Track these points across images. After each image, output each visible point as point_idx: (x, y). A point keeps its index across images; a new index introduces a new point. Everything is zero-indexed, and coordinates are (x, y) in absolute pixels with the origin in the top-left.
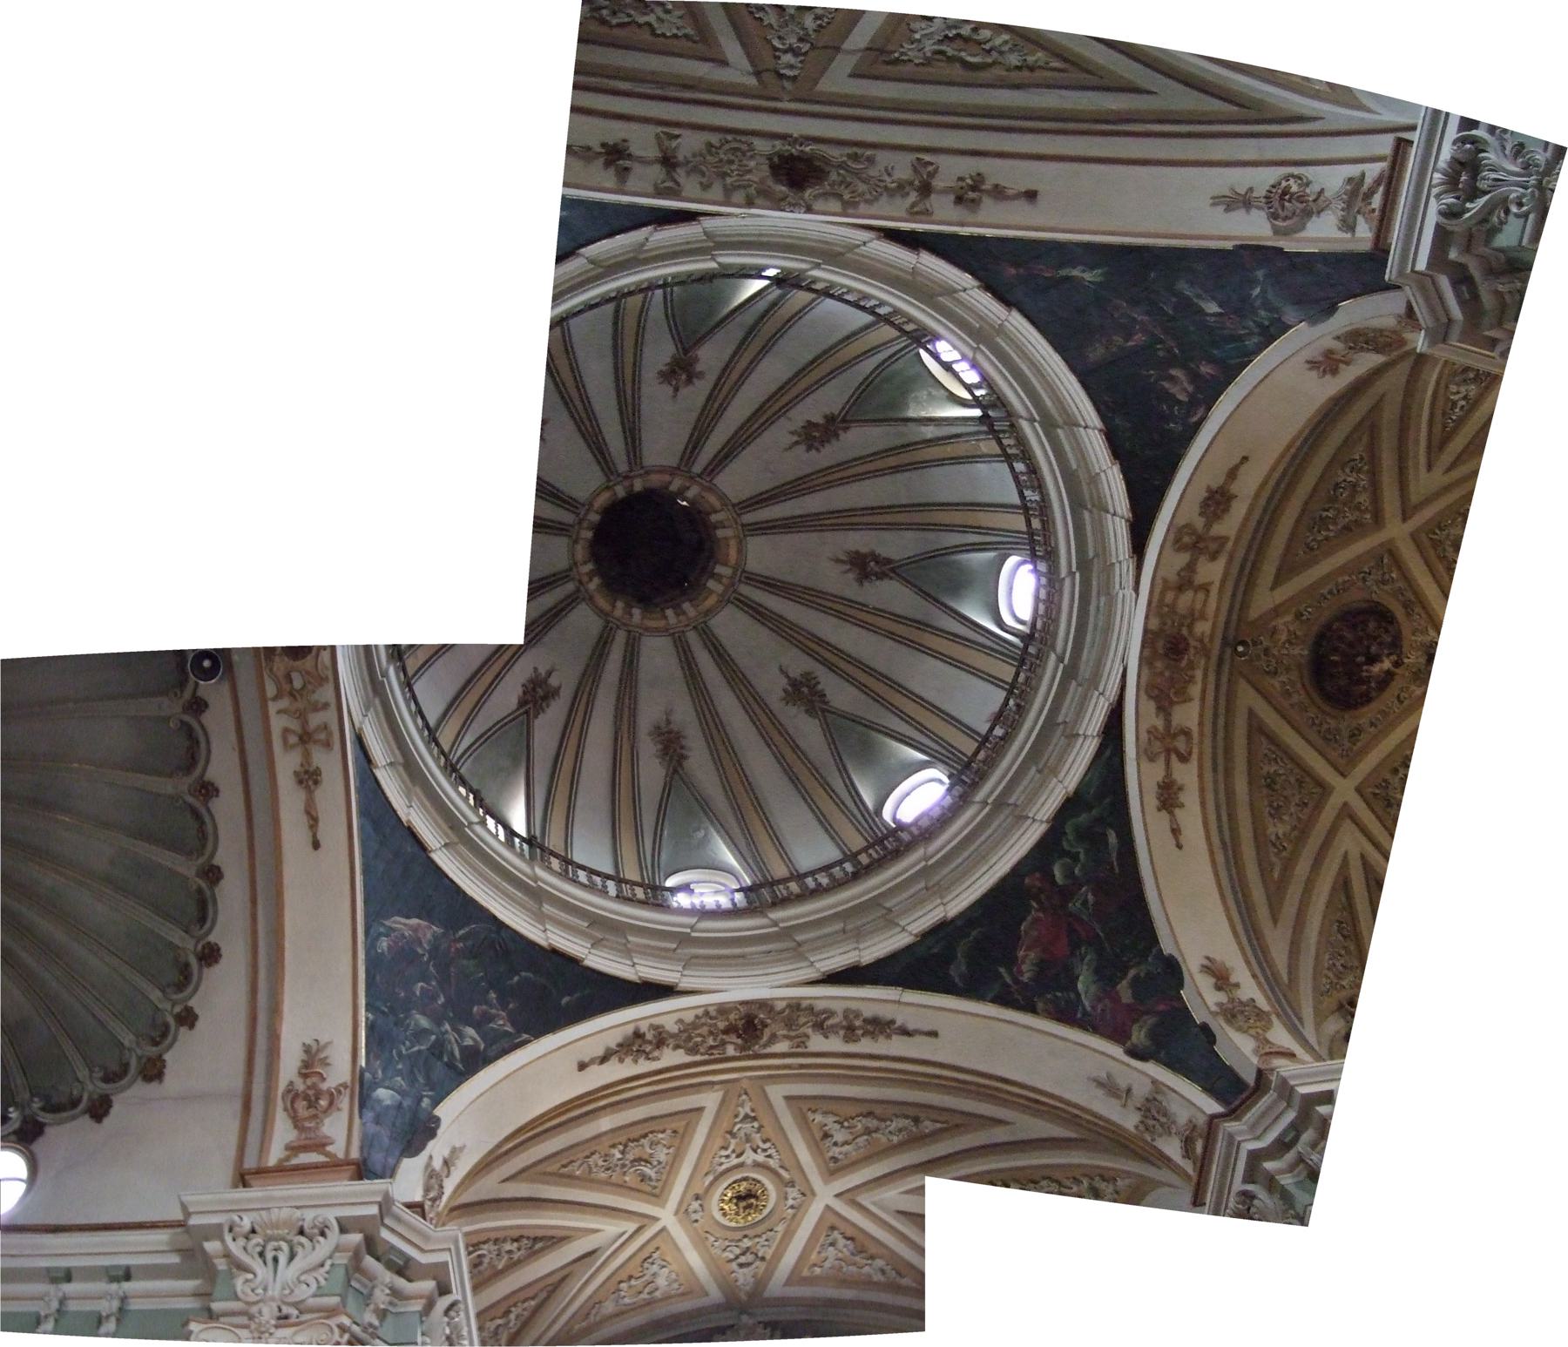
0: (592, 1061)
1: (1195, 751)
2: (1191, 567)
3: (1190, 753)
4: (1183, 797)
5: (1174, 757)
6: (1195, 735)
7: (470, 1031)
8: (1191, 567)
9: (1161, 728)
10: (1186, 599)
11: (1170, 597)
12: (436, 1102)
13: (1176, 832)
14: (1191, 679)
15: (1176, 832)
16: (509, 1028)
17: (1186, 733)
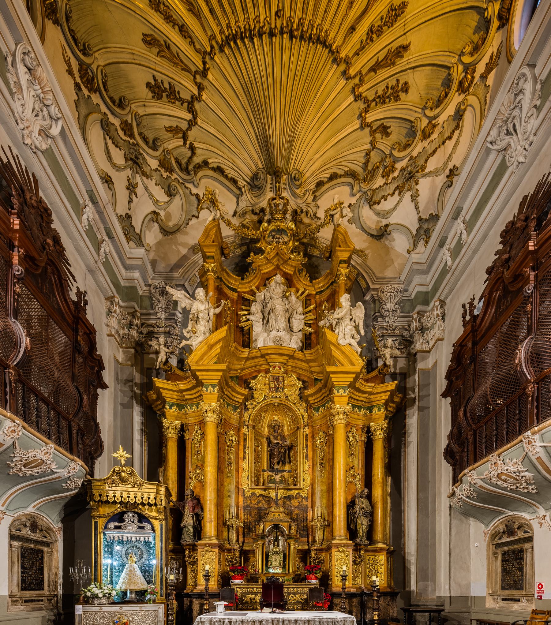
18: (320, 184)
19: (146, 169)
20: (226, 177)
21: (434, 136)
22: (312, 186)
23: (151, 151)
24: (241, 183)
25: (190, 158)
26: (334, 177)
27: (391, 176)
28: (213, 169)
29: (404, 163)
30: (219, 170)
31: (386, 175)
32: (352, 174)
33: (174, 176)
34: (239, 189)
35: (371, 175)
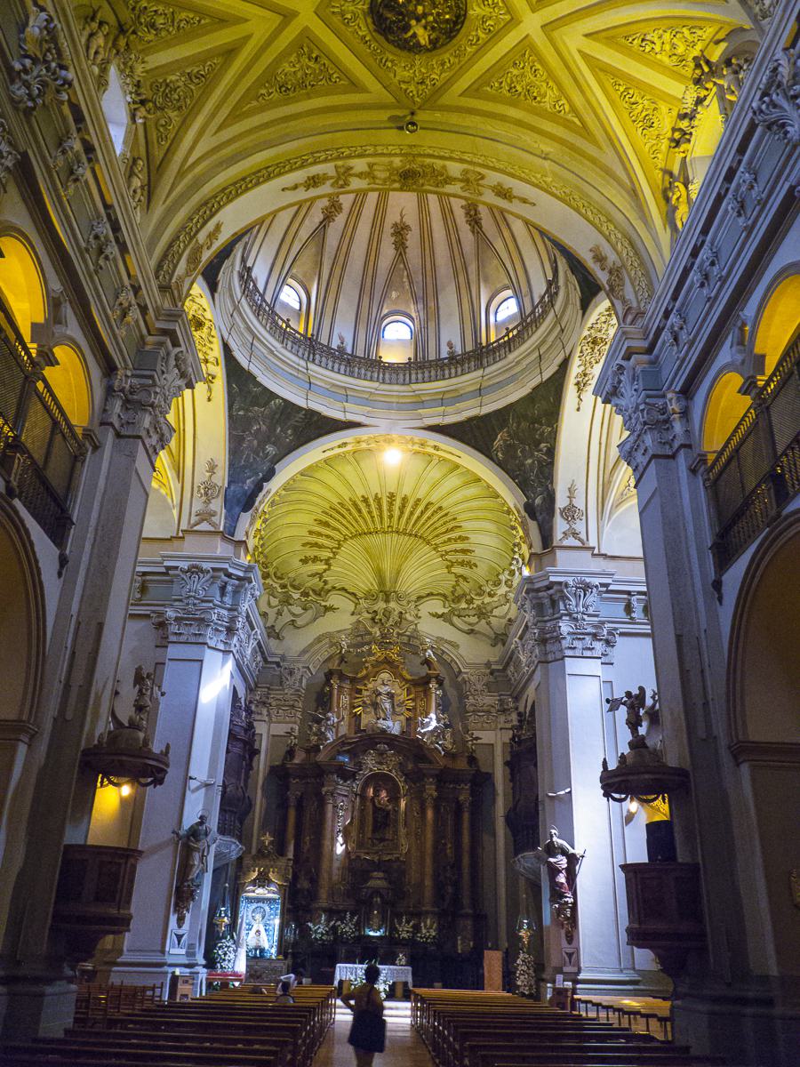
0: (579, 404)
1: (478, 169)
2: (360, 175)
3: (480, 174)
4: (506, 187)
5: (480, 182)
6: (471, 167)
7: (543, 445)
8: (360, 175)
9: (462, 184)
10: (381, 175)
11: (377, 181)
12: (552, 483)
13: (524, 201)
14: (431, 166)
15: (524, 201)
16: (550, 429)
17: (466, 172)
18: (419, 598)
19: (291, 602)
20: (348, 593)
21: (495, 599)
22: (414, 598)
23: (296, 591)
24: (360, 595)
25: (323, 588)
26: (432, 594)
27: (471, 606)
28: (339, 590)
29: (479, 602)
30: (343, 589)
31: (467, 602)
32: (445, 596)
33: (310, 598)
34: (358, 599)
35: (457, 599)
